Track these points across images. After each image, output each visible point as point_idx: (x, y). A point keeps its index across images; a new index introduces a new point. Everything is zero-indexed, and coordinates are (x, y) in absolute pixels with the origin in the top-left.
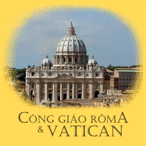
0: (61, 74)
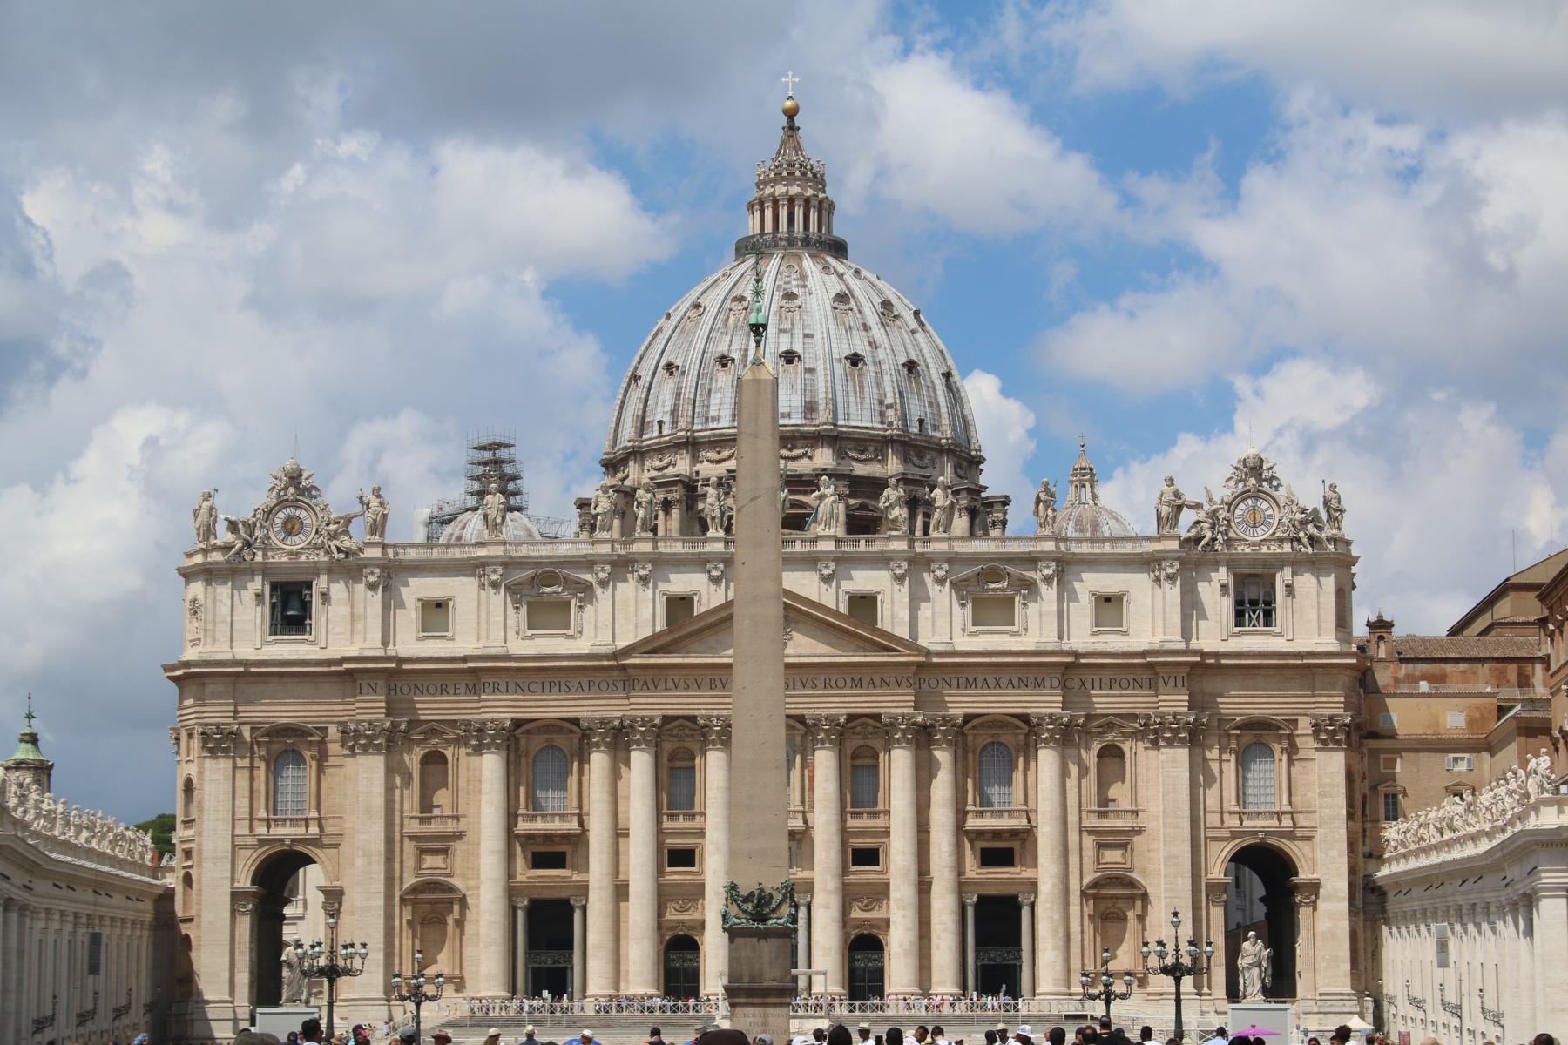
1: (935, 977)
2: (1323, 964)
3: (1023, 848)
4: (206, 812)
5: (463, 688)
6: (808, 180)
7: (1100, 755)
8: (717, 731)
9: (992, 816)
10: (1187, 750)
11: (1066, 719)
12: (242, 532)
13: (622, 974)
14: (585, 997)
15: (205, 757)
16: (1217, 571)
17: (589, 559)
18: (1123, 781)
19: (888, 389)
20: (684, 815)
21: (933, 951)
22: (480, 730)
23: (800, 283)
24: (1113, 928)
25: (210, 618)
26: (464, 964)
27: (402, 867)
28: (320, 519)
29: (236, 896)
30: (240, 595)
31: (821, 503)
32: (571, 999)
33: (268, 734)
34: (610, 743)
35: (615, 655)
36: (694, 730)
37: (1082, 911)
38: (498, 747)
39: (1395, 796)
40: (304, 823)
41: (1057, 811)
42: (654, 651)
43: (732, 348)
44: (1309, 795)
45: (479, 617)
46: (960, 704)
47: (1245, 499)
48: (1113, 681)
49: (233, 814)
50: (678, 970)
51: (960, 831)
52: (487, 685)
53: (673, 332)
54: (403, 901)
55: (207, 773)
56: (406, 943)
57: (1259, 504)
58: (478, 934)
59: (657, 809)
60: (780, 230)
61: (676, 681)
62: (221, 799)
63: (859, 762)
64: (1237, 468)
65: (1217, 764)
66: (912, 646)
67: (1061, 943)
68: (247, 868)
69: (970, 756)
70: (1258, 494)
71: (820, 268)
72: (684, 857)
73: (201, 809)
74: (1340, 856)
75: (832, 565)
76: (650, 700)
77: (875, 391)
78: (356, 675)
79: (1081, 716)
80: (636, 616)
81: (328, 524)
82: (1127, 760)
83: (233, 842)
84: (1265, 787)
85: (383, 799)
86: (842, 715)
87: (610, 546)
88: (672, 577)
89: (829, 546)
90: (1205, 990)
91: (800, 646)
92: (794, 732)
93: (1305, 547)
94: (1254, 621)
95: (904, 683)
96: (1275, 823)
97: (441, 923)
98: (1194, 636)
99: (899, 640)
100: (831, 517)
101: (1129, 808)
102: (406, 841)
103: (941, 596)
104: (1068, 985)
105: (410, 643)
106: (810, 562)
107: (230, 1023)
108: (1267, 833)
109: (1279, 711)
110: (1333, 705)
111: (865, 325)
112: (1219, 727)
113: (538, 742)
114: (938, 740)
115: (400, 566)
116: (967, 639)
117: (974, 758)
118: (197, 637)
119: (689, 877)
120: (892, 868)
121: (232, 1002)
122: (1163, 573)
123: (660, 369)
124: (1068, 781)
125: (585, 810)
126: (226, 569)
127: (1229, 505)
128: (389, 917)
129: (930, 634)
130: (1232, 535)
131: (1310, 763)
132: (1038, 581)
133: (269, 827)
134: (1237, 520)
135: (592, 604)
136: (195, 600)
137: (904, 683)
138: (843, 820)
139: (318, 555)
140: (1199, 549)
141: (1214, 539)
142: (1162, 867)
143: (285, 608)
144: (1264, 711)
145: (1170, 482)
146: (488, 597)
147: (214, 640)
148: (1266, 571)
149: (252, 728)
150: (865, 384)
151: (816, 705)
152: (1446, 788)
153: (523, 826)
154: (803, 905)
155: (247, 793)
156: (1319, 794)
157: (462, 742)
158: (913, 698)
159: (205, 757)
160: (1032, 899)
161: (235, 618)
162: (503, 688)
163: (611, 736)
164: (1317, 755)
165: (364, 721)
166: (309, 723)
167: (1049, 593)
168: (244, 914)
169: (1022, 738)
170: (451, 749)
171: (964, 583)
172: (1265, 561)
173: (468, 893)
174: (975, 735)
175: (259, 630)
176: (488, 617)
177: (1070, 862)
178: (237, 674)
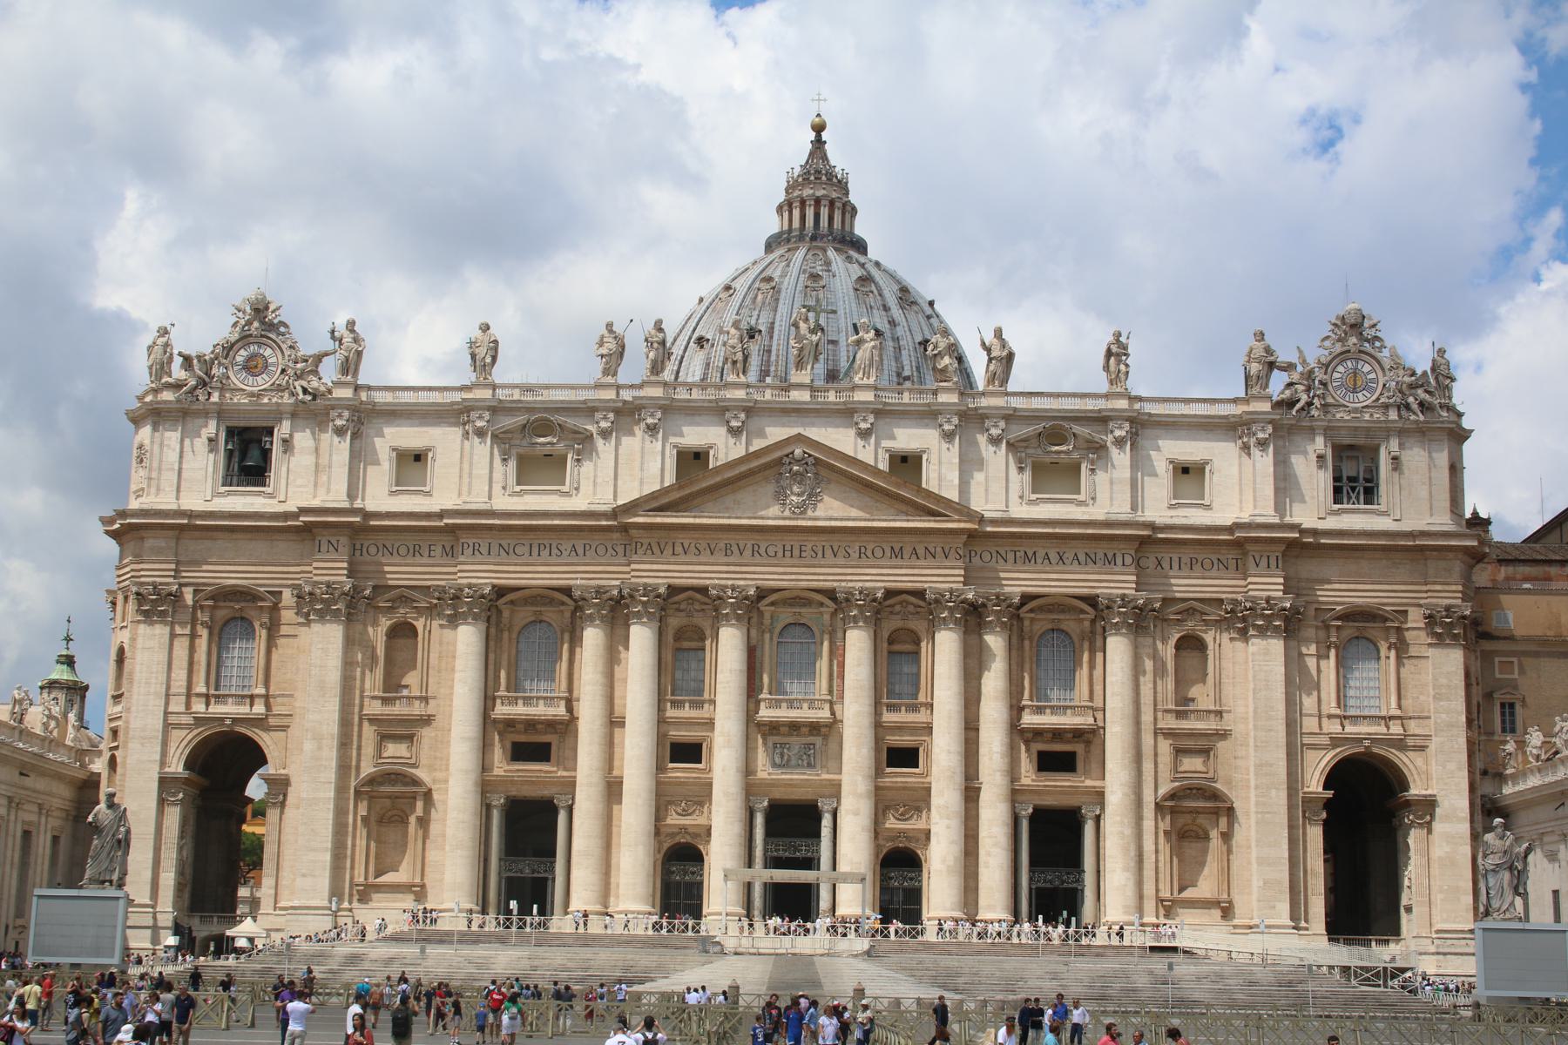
0: (725, 448)
1: (983, 900)
2: (1440, 896)
3: (1087, 752)
4: (136, 685)
5: (439, 550)
6: (833, 185)
7: (1178, 647)
9: (1052, 713)
10: (1282, 642)
11: (1141, 602)
12: (196, 368)
13: (613, 886)
14: (566, 913)
15: (139, 622)
16: (1313, 440)
17: (589, 404)
18: (1203, 680)
19: (906, 362)
20: (690, 702)
22: (456, 597)
23: (825, 268)
24: (1191, 849)
25: (155, 464)
26: (427, 869)
27: (359, 755)
28: (287, 358)
29: (165, 782)
30: (192, 444)
31: (859, 349)
35: (615, 513)
37: (1157, 828)
38: (476, 617)
39: (1512, 706)
40: (248, 701)
41: (1129, 709)
42: (661, 509)
43: (760, 321)
44: (1422, 698)
45: (461, 470)
46: (1017, 582)
47: (1345, 360)
48: (1194, 562)
49: (168, 687)
50: (679, 884)
51: (1017, 733)
52: (466, 545)
53: (705, 312)
54: (358, 793)
55: (140, 641)
56: (360, 842)
57: (1360, 367)
58: (444, 836)
59: (659, 694)
60: (807, 225)
61: (686, 546)
62: (155, 670)
63: (897, 647)
64: (1335, 325)
65: (1315, 660)
66: (963, 510)
67: (1132, 864)
68: (179, 751)
69: (1027, 643)
72: (689, 752)
73: (131, 682)
74: (1460, 769)
75: (871, 419)
76: (655, 567)
77: (893, 364)
78: (314, 530)
80: (642, 470)
81: (296, 363)
82: (1210, 653)
83: (165, 720)
84: (1369, 688)
85: (339, 673)
86: (880, 588)
87: (614, 392)
88: (685, 429)
89: (868, 396)
90: (1303, 924)
91: (832, 508)
92: (822, 609)
93: (1414, 413)
94: (1353, 496)
95: (953, 554)
96: (1383, 729)
97: (402, 822)
98: (1288, 513)
99: (948, 502)
100: (871, 365)
101: (1212, 708)
102: (366, 724)
103: (997, 459)
104: (1140, 910)
105: (380, 497)
106: (846, 413)
107: (149, 932)
109: (1386, 600)
110: (1448, 595)
111: (884, 306)
112: (1316, 618)
113: (525, 615)
114: (990, 622)
117: (1031, 647)
118: (141, 486)
119: (694, 775)
120: (935, 770)
122: (1253, 440)
123: (691, 344)
124: (1142, 679)
125: (575, 694)
126: (178, 410)
127: (1327, 366)
128: (340, 812)
130: (1330, 400)
131: (1423, 661)
132: (1109, 444)
133: (208, 704)
134: (1334, 384)
136: (140, 447)
137: (953, 554)
138: (877, 713)
139: (282, 397)
140: (1294, 413)
142: (1252, 776)
143: (244, 455)
144: (1368, 600)
146: (472, 447)
147: (158, 489)
148: (1369, 442)
149: (195, 590)
150: (885, 357)
153: (501, 710)
154: (828, 812)
155: (185, 664)
156: (1434, 697)
157: (435, 612)
158: (962, 572)
159: (139, 622)
160: (1098, 812)
161: (184, 466)
162: (484, 550)
163: (608, 608)
164: (1431, 652)
165: (322, 583)
166: (261, 586)
167: (1121, 459)
168: (173, 804)
169: (1087, 624)
170: (422, 620)
172: (1368, 429)
174: (1032, 620)
175: (210, 481)
177: (1144, 769)
178: (181, 527)
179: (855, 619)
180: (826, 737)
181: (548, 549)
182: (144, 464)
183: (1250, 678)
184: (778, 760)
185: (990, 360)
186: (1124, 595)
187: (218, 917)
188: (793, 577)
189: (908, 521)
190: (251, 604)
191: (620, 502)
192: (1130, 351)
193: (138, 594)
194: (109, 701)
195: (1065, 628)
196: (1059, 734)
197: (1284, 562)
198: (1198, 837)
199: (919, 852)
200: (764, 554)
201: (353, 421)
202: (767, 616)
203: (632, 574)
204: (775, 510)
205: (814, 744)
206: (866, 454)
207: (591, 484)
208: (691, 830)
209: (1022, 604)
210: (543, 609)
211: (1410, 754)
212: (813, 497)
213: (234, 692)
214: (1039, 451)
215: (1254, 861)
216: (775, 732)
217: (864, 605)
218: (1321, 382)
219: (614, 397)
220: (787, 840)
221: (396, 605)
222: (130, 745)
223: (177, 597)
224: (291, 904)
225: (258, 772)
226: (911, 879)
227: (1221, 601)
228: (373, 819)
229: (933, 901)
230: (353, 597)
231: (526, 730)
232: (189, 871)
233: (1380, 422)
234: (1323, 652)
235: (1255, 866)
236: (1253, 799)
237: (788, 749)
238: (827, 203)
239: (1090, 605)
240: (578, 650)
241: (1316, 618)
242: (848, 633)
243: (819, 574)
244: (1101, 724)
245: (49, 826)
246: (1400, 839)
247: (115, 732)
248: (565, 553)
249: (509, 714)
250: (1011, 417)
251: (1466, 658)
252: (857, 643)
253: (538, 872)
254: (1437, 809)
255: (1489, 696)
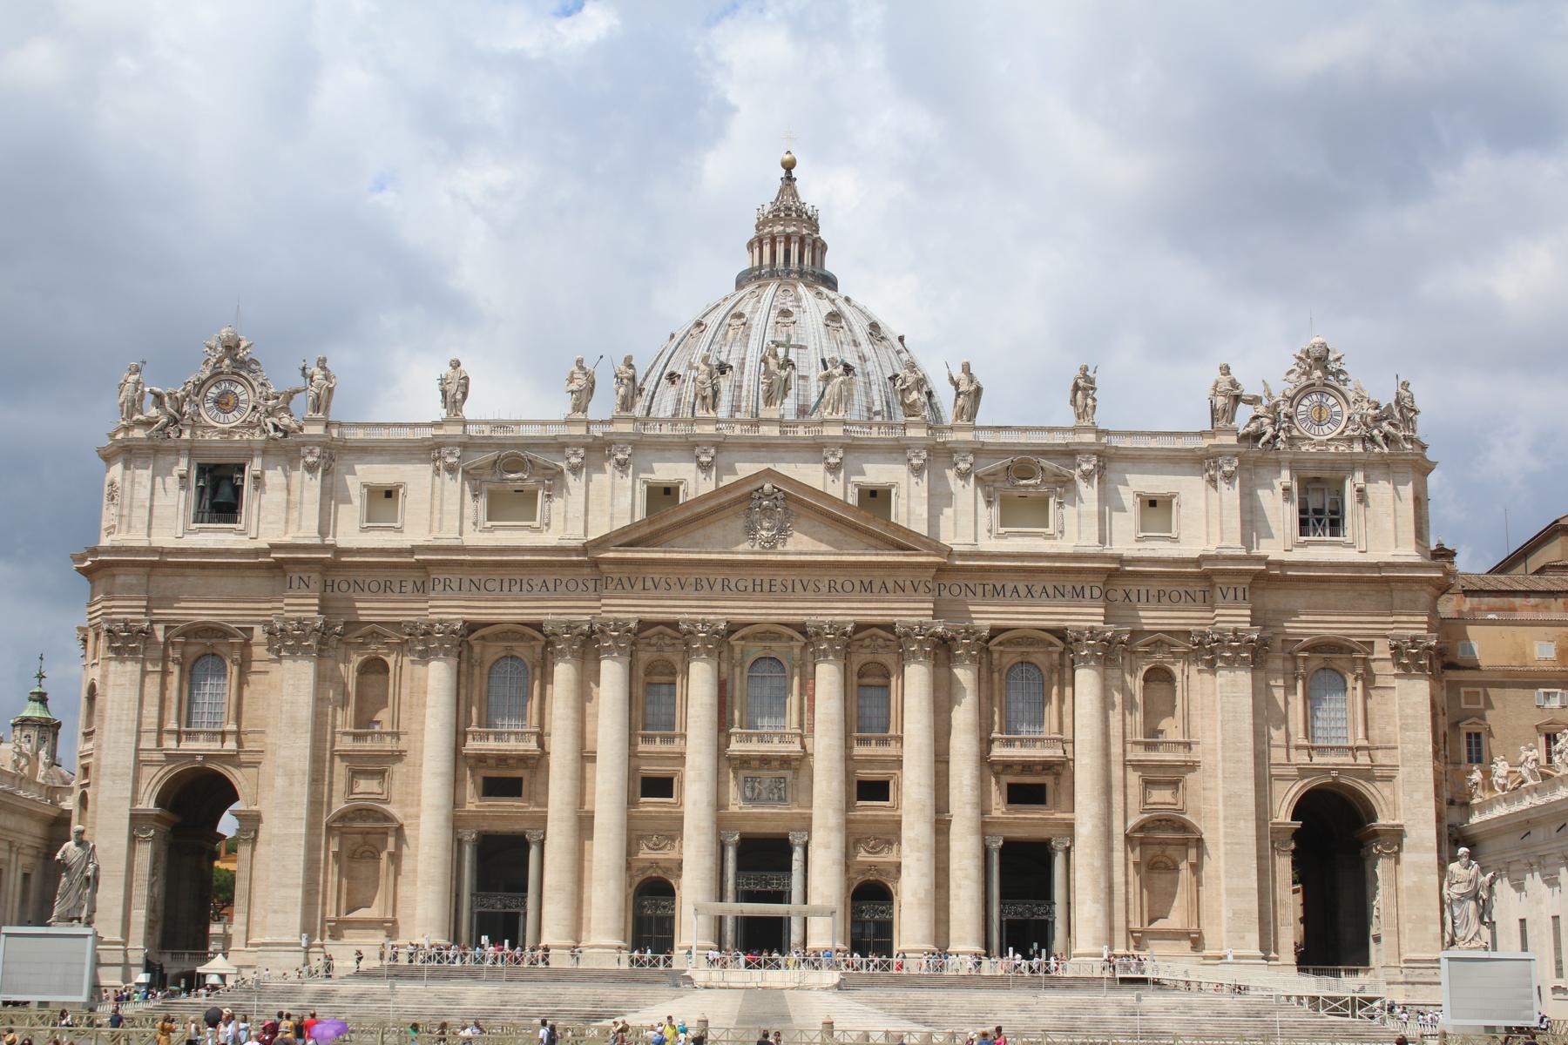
0: (694, 482)
3: (1057, 784)
4: (107, 720)
5: (409, 586)
6: (803, 221)
7: (1146, 679)
8: (702, 637)
9: (1022, 746)
10: (1249, 675)
11: (1110, 634)
12: (167, 405)
13: (585, 921)
15: (110, 659)
17: (560, 440)
18: (1172, 713)
19: (876, 397)
21: (951, 902)
22: (427, 633)
24: (1161, 880)
25: (126, 502)
26: (399, 906)
27: (331, 791)
28: (258, 394)
29: (137, 819)
32: (523, 949)
33: (184, 634)
34: (577, 651)
35: (585, 549)
36: (676, 638)
37: (1126, 859)
39: (1478, 735)
40: (219, 737)
42: (631, 544)
46: (986, 615)
49: (140, 724)
50: (650, 918)
51: (987, 765)
53: (676, 348)
54: (329, 829)
55: (111, 679)
56: (331, 877)
57: (1324, 400)
58: (415, 871)
61: (656, 581)
62: (126, 706)
63: (866, 681)
64: (1300, 358)
65: (1282, 691)
66: (932, 544)
67: (1102, 896)
68: (150, 788)
69: (996, 676)
70: (1324, 389)
71: (814, 293)
72: (660, 786)
73: (102, 719)
74: (1426, 799)
75: (840, 454)
77: (864, 399)
78: (285, 567)
79: (1125, 632)
80: (612, 505)
81: (267, 400)
82: (1178, 684)
83: (137, 756)
84: (1337, 719)
86: (850, 622)
87: (585, 428)
88: (656, 466)
90: (1273, 955)
92: (792, 643)
93: (1379, 446)
95: (922, 588)
100: (840, 400)
101: (1181, 739)
102: (337, 760)
103: (965, 493)
105: (351, 532)
106: (815, 449)
107: (119, 970)
108: (1341, 771)
110: (1414, 626)
111: (854, 341)
112: (1283, 650)
113: (495, 650)
115: (344, 447)
116: (994, 541)
117: (1000, 679)
118: (113, 523)
120: (905, 803)
121: (125, 944)
122: (1219, 475)
123: (663, 379)
125: (547, 729)
126: (150, 448)
127: (1292, 399)
128: (312, 848)
129: (952, 534)
130: (1295, 433)
131: (1389, 691)
132: (1076, 477)
133: (179, 741)
135: (562, 497)
136: (112, 484)
137: (922, 588)
138: (848, 747)
140: (1260, 446)
141: (1275, 437)
145: (1226, 370)
146: (443, 483)
147: (129, 527)
149: (166, 627)
150: (855, 393)
151: (819, 612)
152: (1537, 726)
153: (473, 746)
154: (798, 845)
155: (156, 701)
156: (1401, 728)
157: (406, 648)
158: (931, 606)
161: (156, 503)
162: (455, 586)
163: (579, 643)
164: (1396, 683)
167: (1089, 493)
168: (145, 841)
169: (1056, 656)
170: (393, 656)
171: (992, 478)
172: (1333, 462)
173: (405, 823)
174: (1002, 652)
176: (442, 505)
178: (152, 564)
179: (825, 653)
180: (796, 770)
181: (519, 584)
182: (115, 502)
183: (1219, 711)
184: (748, 794)
185: (958, 394)
186: (1093, 627)
187: (190, 954)
188: (764, 611)
189: (877, 555)
190: (221, 641)
191: (591, 538)
192: (1096, 385)
193: (109, 631)
194: (80, 738)
195: (1034, 661)
196: (1029, 767)
197: (1251, 594)
198: (1167, 868)
199: (890, 885)
200: (734, 588)
201: (324, 457)
202: (737, 650)
203: (603, 609)
204: (746, 546)
205: (784, 778)
206: (835, 488)
207: (562, 519)
208: (662, 865)
209: (992, 637)
210: (514, 644)
211: (1378, 784)
212: (783, 531)
213: (205, 729)
214: (1008, 485)
215: (1223, 892)
216: (745, 765)
217: (834, 639)
218: (1286, 415)
219: (584, 433)
220: (759, 874)
221: (367, 641)
222: (102, 782)
223: (148, 634)
224: (263, 940)
225: (230, 808)
226: (883, 912)
227: (1188, 633)
228: (344, 855)
229: (903, 934)
230: (324, 633)
231: (497, 765)
232: (160, 908)
233: (1345, 454)
234: (1290, 682)
235: (1224, 897)
236: (1222, 831)
237: (759, 783)
238: (797, 239)
239: (1059, 638)
240: (549, 687)
241: (1283, 650)
242: (818, 667)
243: (725, 607)
244: (1070, 756)
245: (20, 864)
246: (1369, 870)
247: (86, 769)
248: (536, 588)
249: (480, 750)
250: (979, 451)
251: (1431, 688)
252: (827, 677)
253: (510, 907)
254: (1405, 840)
255: (1455, 726)
